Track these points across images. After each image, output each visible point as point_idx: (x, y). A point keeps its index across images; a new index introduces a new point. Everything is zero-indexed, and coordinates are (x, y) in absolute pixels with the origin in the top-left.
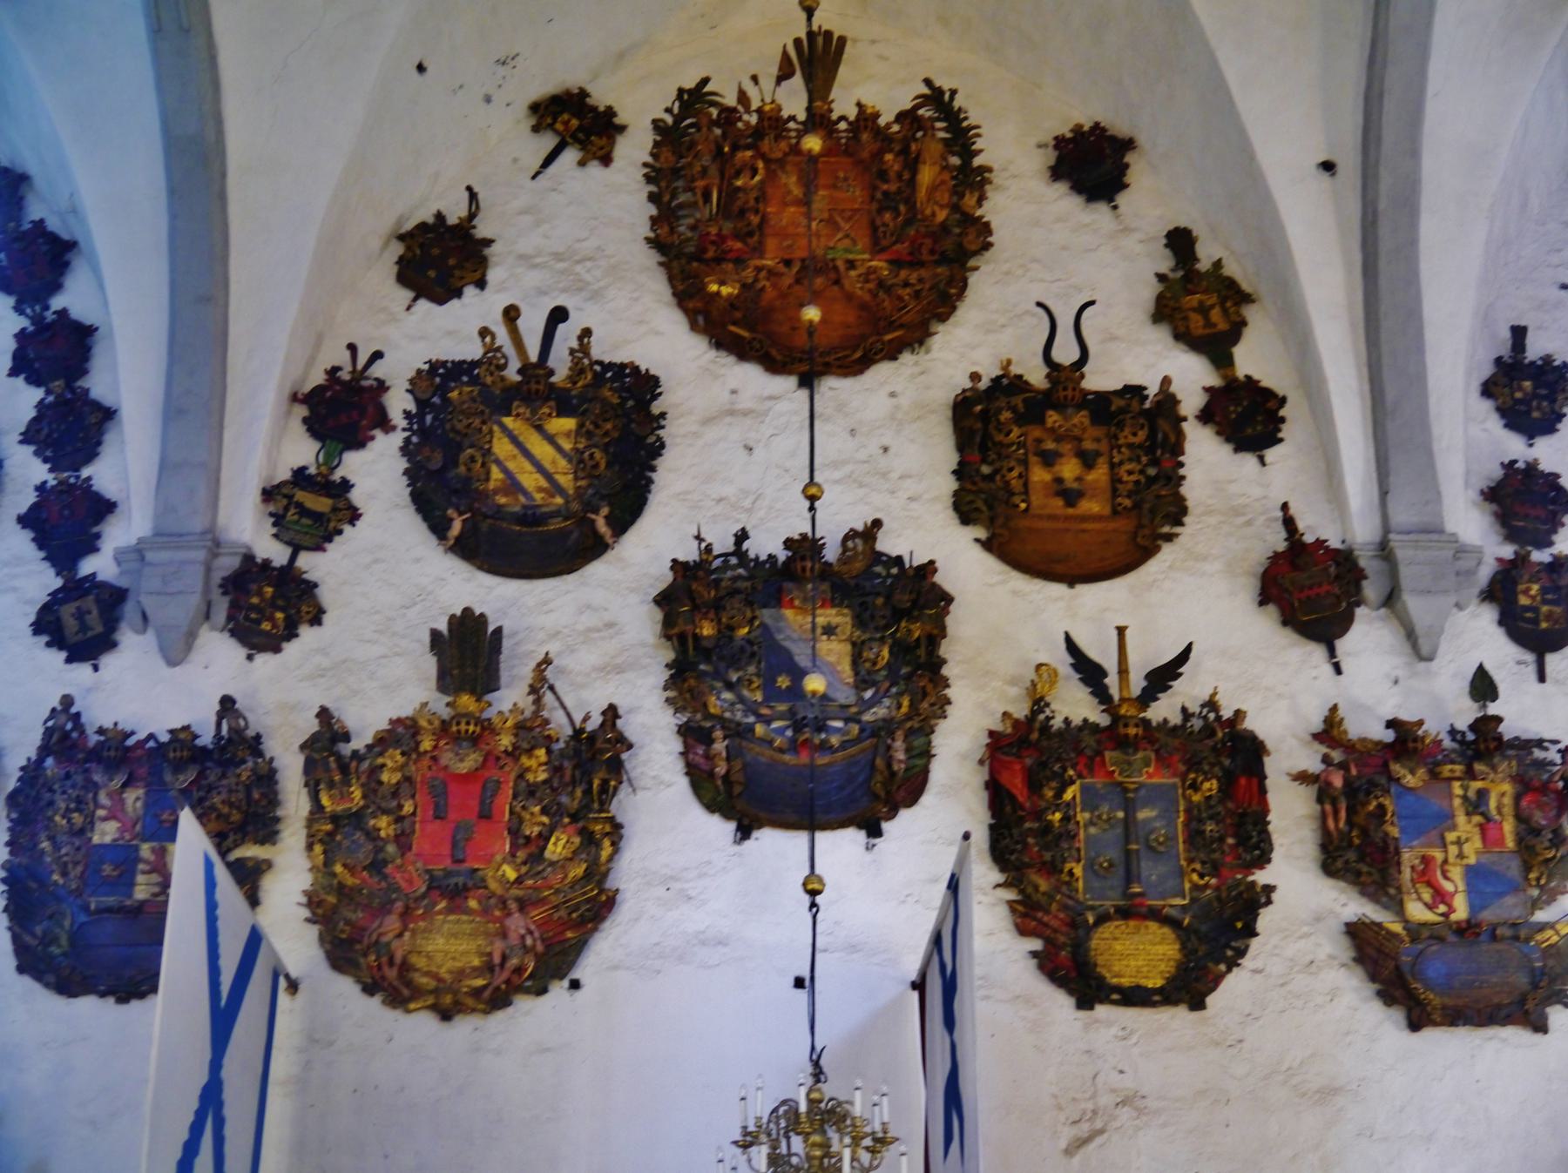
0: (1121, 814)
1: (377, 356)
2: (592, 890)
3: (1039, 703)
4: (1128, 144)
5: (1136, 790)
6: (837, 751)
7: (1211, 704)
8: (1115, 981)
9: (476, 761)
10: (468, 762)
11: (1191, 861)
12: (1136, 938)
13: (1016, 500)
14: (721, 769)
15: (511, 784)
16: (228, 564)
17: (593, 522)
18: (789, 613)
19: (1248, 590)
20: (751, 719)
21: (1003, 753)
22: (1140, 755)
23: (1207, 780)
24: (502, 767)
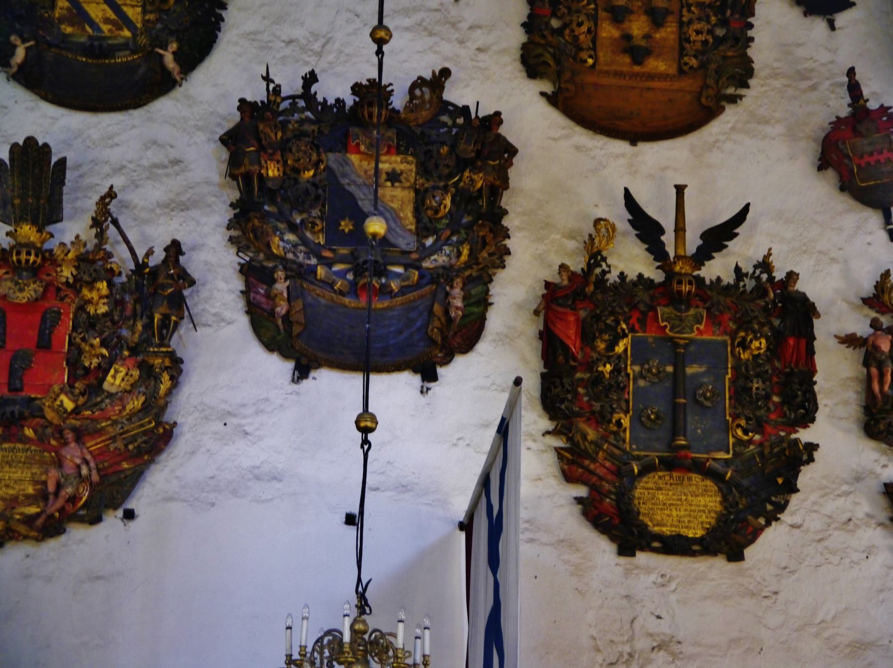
0: (670, 369)
2: (150, 422)
3: (596, 257)
5: (686, 346)
6: (396, 295)
7: (765, 265)
8: (656, 529)
9: (35, 291)
10: (30, 291)
11: (735, 417)
12: (679, 488)
13: (584, 55)
14: (282, 308)
15: (71, 316)
17: (161, 57)
18: (354, 158)
19: (809, 152)
20: (314, 261)
21: (559, 305)
22: (692, 311)
23: (756, 338)
24: (62, 299)
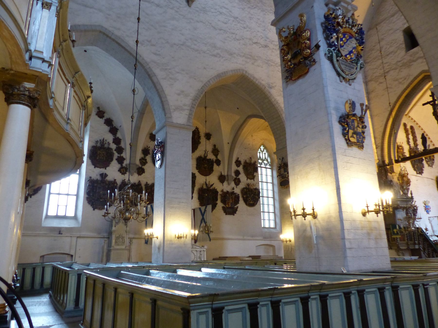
1: (149, 147)
3: (203, 187)
4: (211, 135)
16: (137, 167)
